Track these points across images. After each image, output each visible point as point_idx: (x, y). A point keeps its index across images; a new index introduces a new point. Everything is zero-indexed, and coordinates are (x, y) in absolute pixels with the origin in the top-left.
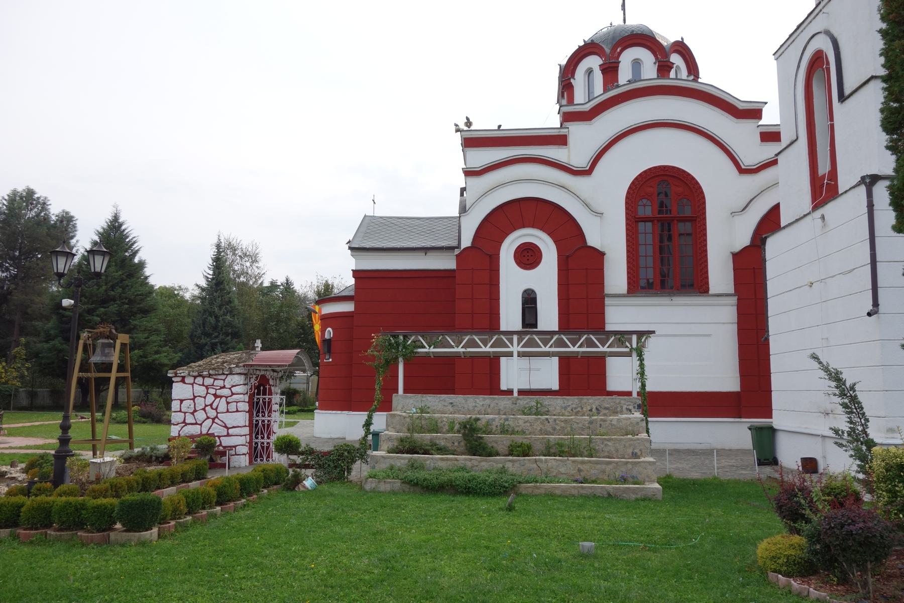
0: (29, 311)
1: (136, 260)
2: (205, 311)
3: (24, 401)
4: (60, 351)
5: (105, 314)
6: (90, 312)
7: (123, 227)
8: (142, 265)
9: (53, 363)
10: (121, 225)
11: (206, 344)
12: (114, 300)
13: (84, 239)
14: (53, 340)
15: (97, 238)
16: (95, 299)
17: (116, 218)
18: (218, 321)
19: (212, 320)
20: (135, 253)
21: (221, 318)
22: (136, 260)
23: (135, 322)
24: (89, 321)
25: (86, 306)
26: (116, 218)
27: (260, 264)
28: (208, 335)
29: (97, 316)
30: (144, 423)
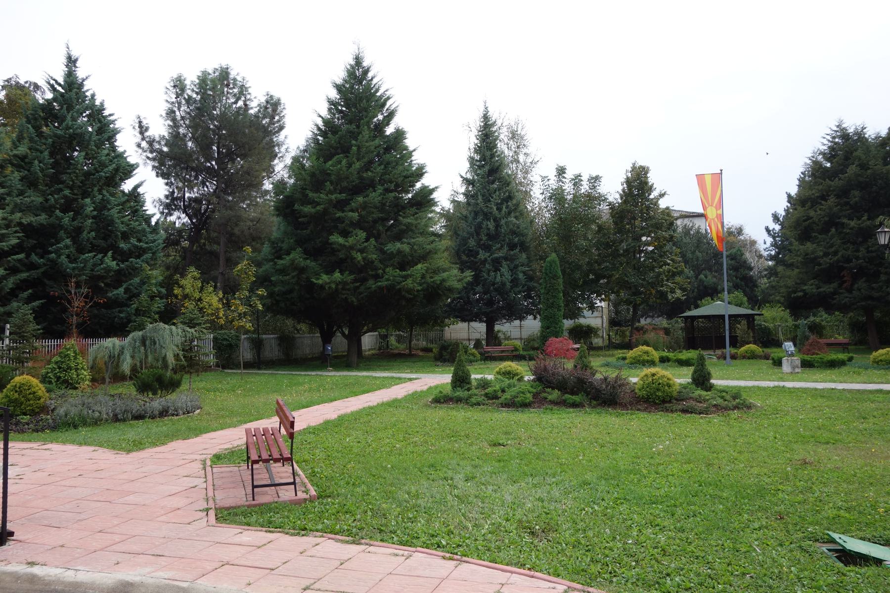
0: (236, 231)
1: (389, 130)
2: (476, 214)
3: (246, 353)
4: (302, 270)
5: (364, 206)
6: (341, 205)
7: (370, 75)
8: (400, 135)
9: (291, 291)
10: (366, 72)
11: (486, 260)
12: (372, 185)
13: (297, 134)
14: (288, 254)
15: (334, 94)
16: (345, 184)
17: (358, 61)
18: (498, 226)
19: (491, 225)
20: (391, 115)
21: (503, 222)
22: (389, 130)
23: (409, 221)
24: (340, 220)
25: (333, 197)
26: (358, 61)
27: (531, 149)
28: (487, 248)
29: (352, 211)
30: (574, 405)
